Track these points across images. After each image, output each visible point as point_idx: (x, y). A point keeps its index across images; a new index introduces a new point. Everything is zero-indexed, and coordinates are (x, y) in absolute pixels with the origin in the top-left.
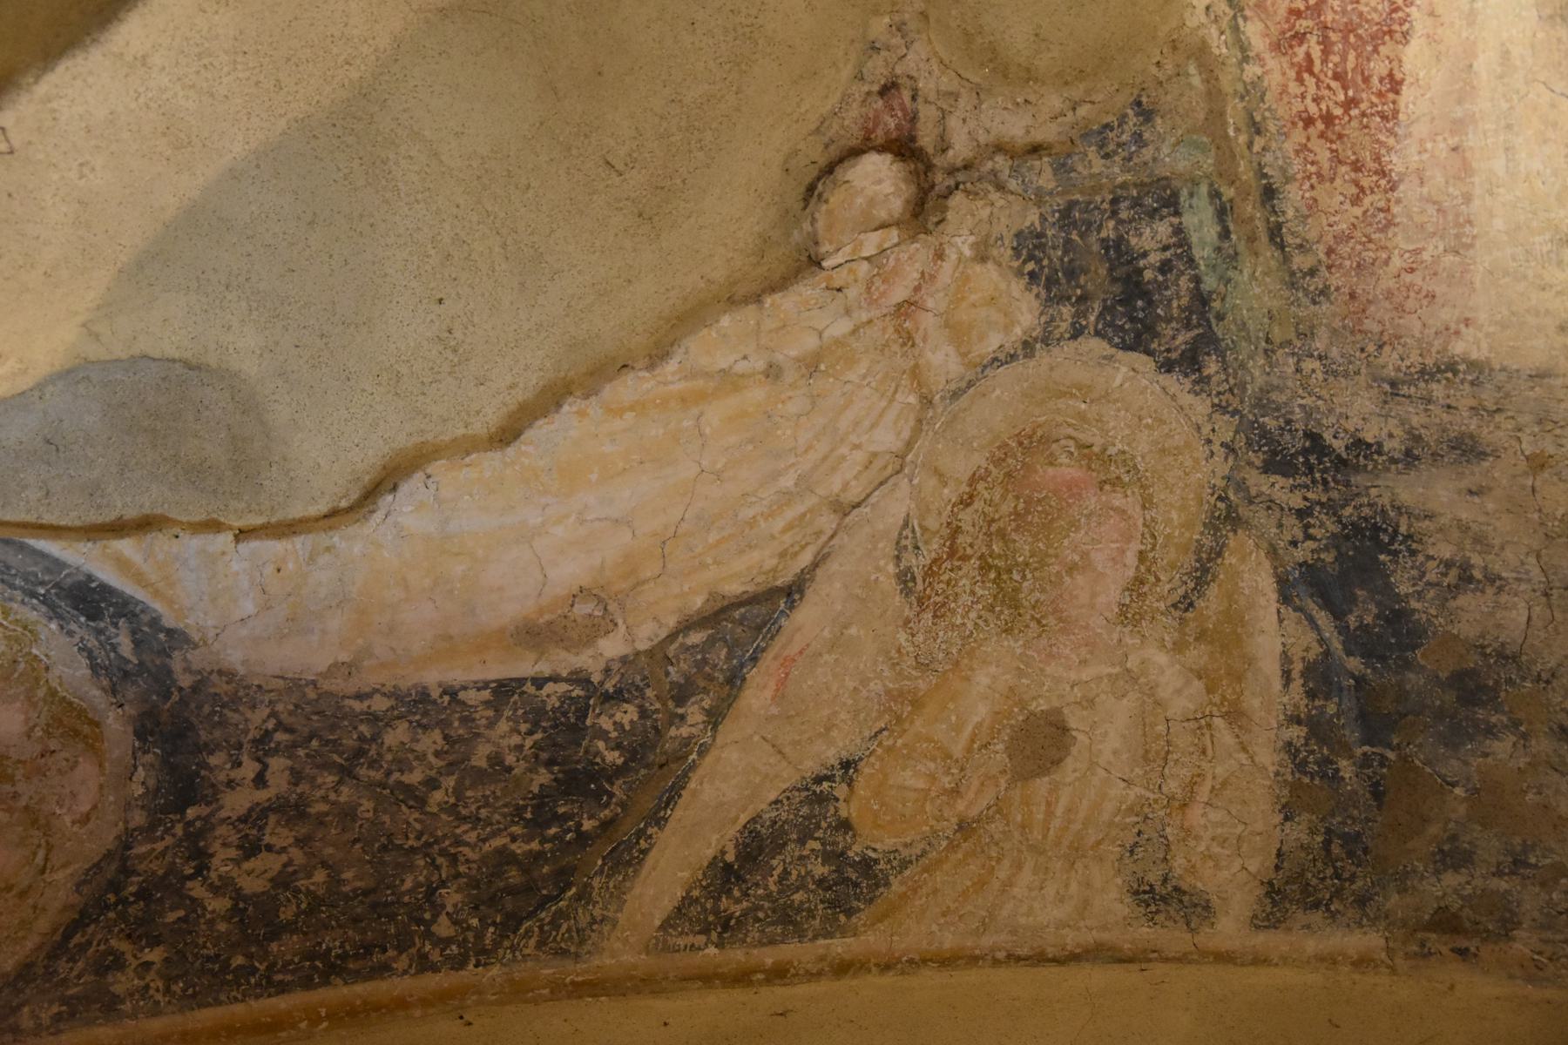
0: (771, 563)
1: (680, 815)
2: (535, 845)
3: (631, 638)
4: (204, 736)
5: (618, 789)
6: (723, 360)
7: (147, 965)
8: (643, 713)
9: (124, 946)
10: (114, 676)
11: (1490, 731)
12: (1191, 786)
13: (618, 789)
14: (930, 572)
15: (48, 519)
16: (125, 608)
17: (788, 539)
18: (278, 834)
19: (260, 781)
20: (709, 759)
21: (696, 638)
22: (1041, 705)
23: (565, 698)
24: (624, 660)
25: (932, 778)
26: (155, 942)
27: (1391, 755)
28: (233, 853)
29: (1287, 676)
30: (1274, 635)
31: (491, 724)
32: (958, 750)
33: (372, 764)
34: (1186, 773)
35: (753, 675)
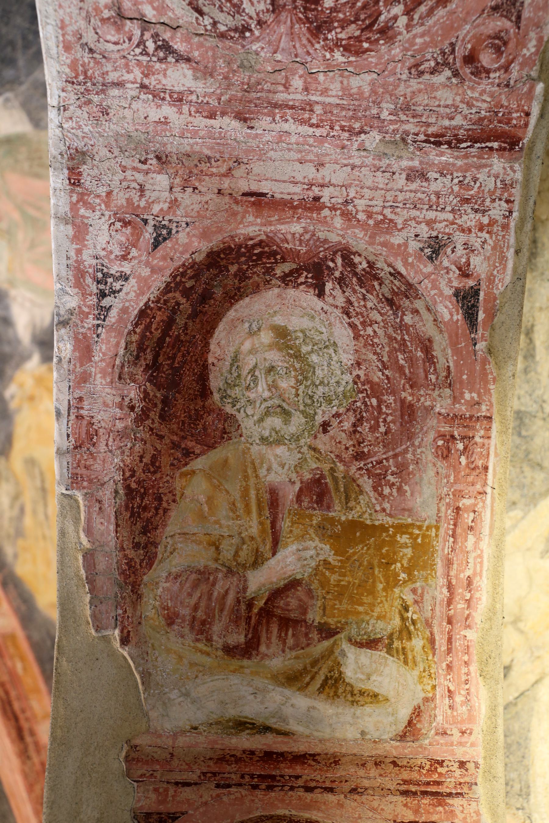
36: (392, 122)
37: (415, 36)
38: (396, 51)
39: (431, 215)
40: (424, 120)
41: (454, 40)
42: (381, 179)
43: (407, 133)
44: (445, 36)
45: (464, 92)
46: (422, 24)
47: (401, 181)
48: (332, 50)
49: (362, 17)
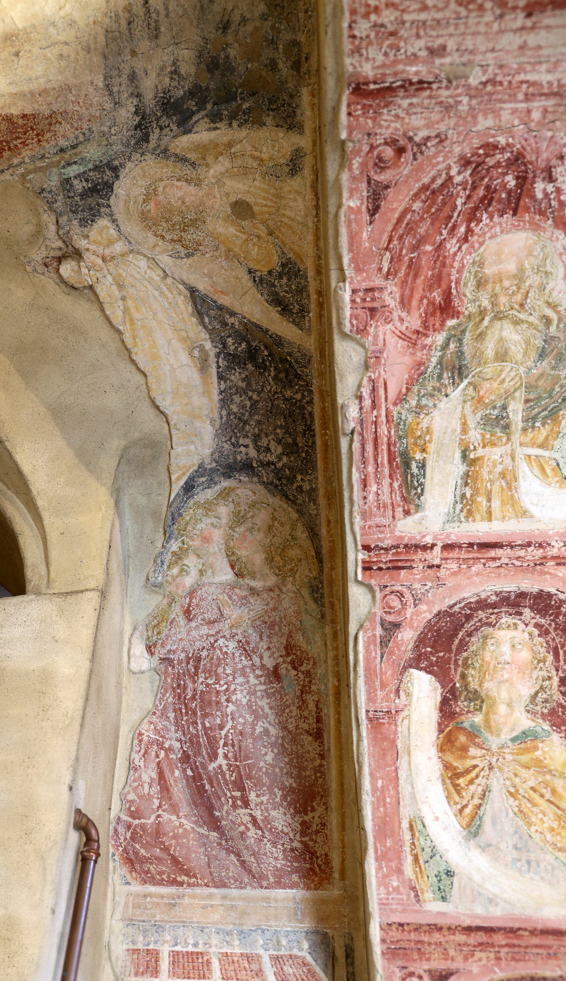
0: (182, 297)
1: (265, 324)
2: (272, 369)
3: (205, 340)
4: (231, 461)
5: (254, 344)
6: (120, 313)
7: (302, 479)
8: (230, 336)
9: (295, 485)
10: (211, 482)
11: (227, 57)
12: (255, 158)
13: (254, 344)
14: (186, 248)
15: (167, 495)
16: (192, 479)
17: (175, 293)
18: (264, 442)
19: (246, 446)
20: (247, 316)
21: (207, 320)
22: (229, 210)
23: (224, 359)
24: (212, 342)
25: (254, 244)
26: (295, 477)
27: (240, 90)
28: (269, 455)
29: (216, 129)
30: (202, 135)
31: (232, 381)
32: (244, 237)
33: (243, 415)
34: (250, 161)
35: (220, 301)
36: (460, 95)
37: (444, 162)
38: (457, 150)
39: (423, 16)
40: (434, 101)
41: (415, 163)
42: (469, 43)
43: (447, 88)
44: (422, 164)
45: (402, 126)
46: (439, 171)
47: (451, 45)
48: (508, 145)
49: (484, 172)
